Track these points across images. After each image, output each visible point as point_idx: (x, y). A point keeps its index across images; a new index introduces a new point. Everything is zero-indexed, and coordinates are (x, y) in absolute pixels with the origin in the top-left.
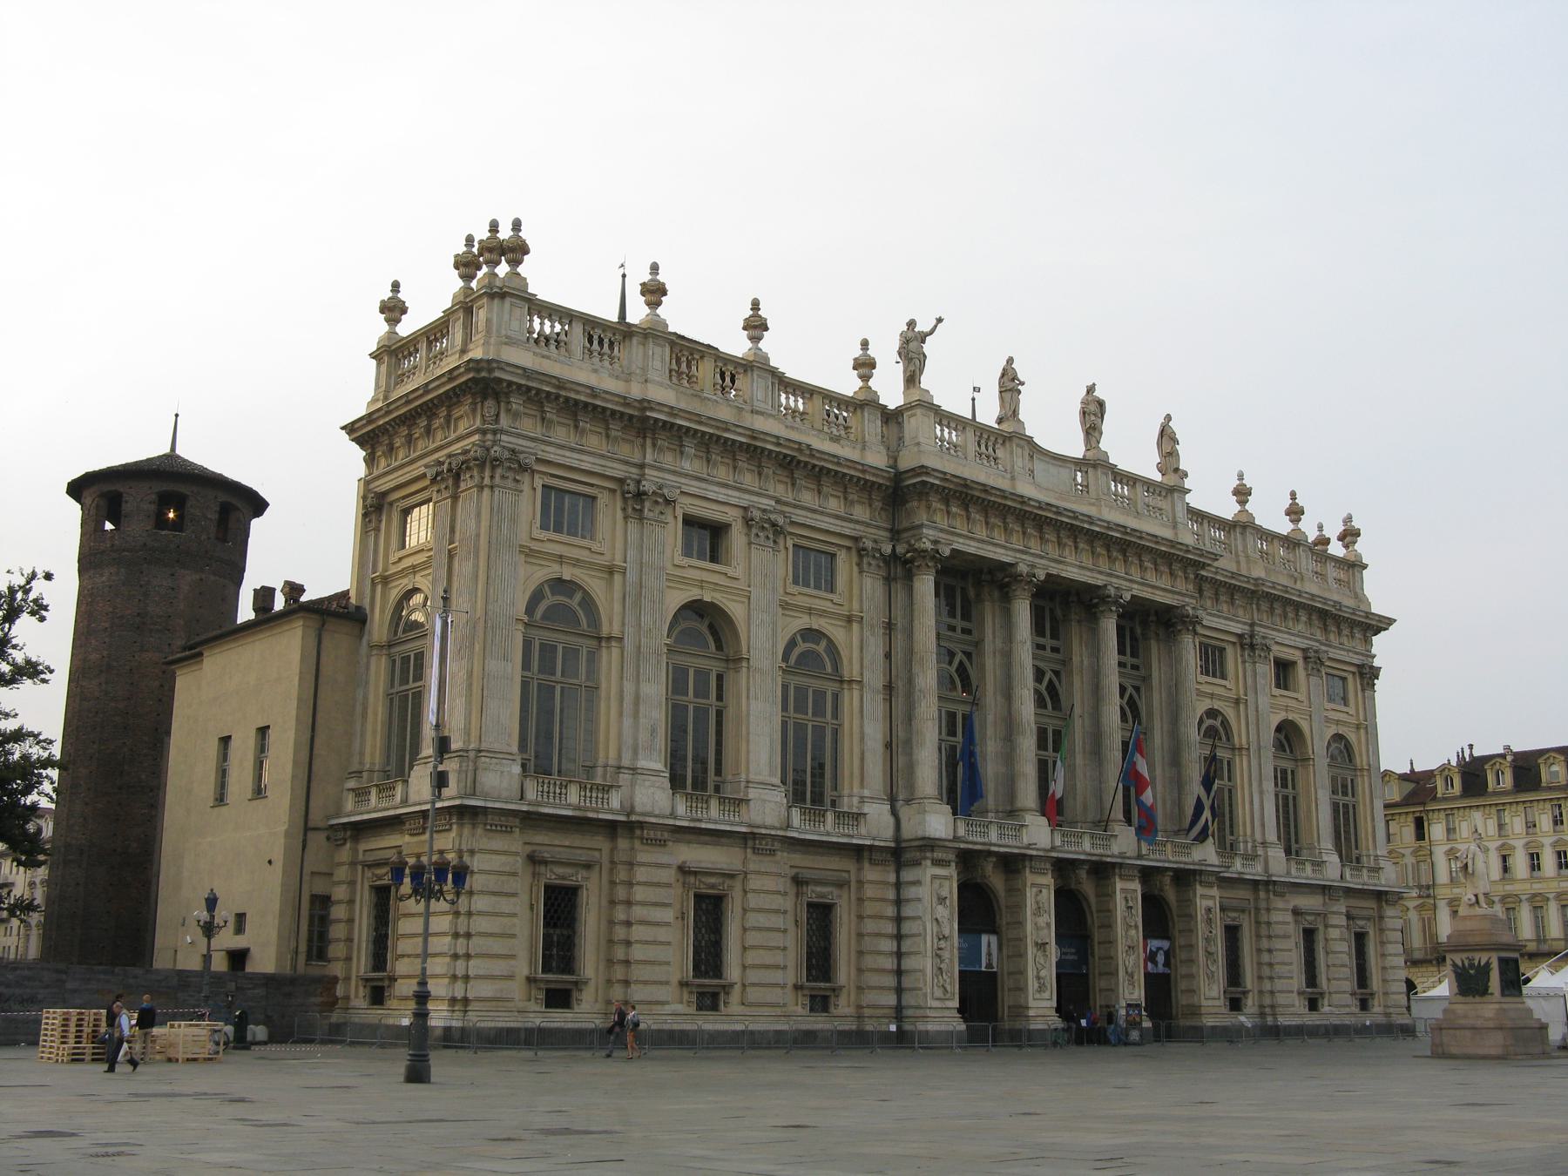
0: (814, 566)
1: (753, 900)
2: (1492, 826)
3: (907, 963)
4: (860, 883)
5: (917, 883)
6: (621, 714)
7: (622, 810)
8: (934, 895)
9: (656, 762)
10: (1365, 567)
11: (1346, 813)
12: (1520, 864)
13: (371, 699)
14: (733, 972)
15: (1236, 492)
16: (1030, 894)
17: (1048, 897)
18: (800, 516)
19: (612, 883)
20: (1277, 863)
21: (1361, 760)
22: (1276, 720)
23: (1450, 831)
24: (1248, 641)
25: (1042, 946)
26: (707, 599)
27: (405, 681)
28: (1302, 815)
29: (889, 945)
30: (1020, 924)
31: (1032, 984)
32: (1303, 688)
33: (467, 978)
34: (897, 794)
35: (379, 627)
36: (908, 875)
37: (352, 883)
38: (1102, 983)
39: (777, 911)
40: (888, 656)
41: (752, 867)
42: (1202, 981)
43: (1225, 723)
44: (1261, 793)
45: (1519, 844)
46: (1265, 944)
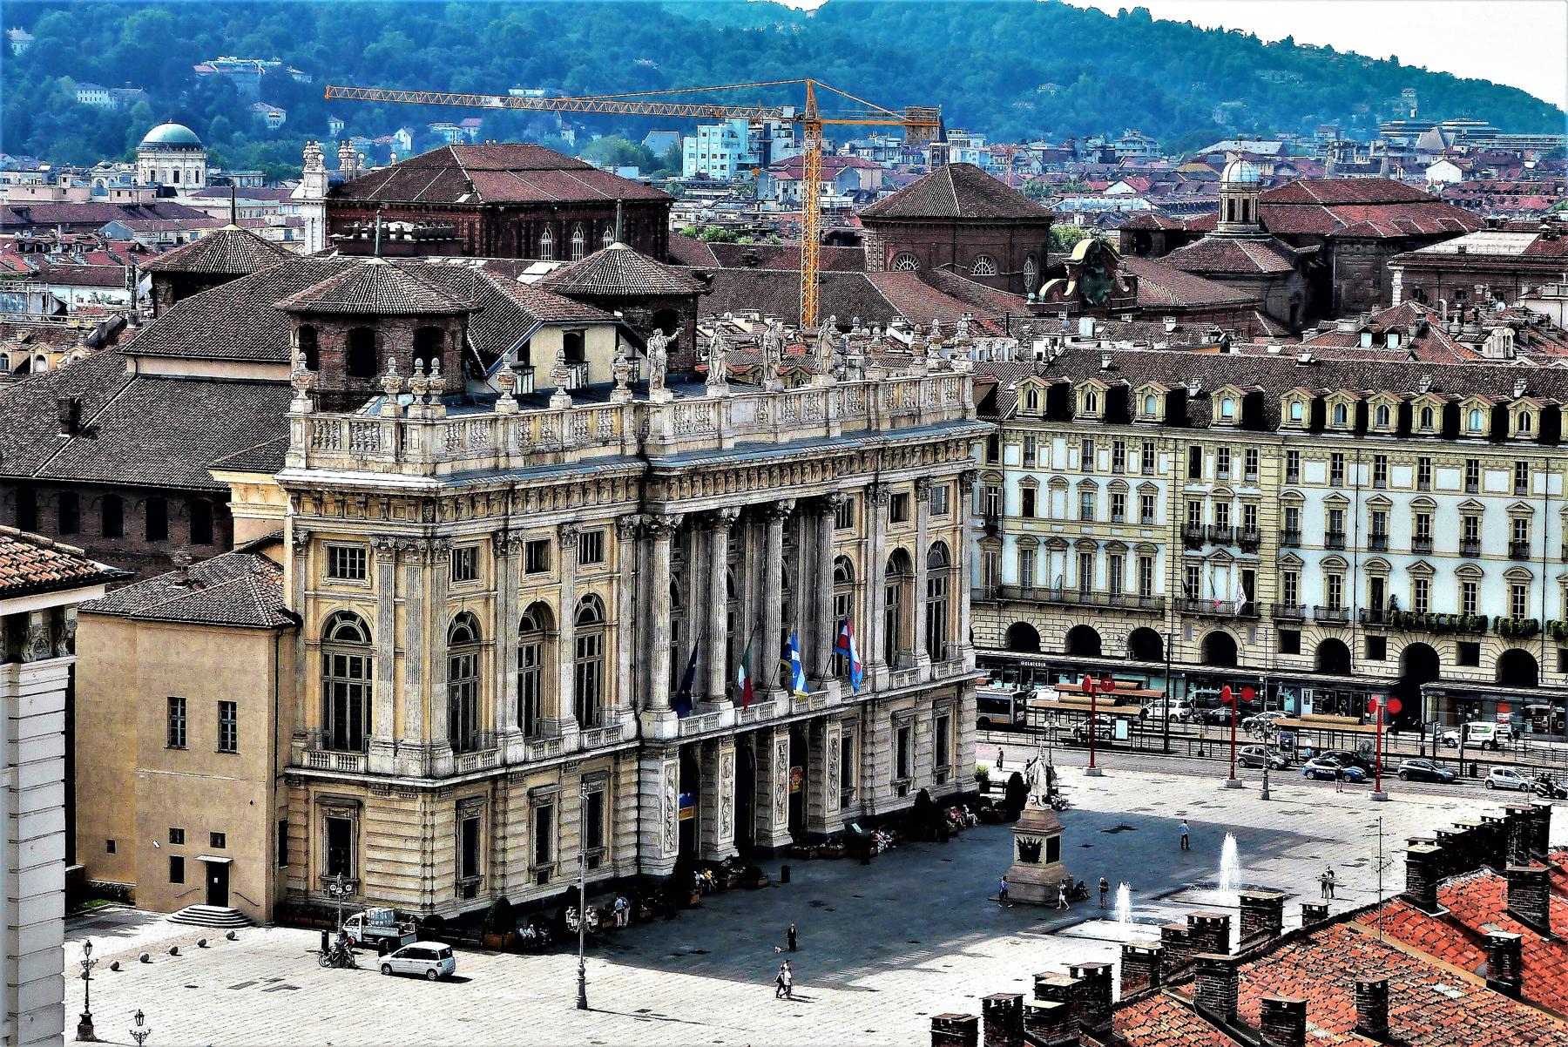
0: (591, 548)
2: (1076, 456)
3: (645, 827)
4: (617, 775)
5: (656, 771)
6: (495, 697)
8: (665, 778)
9: (512, 727)
11: (938, 610)
12: (1102, 510)
13: (309, 682)
14: (554, 856)
16: (721, 762)
17: (732, 760)
19: (495, 813)
23: (1028, 456)
25: (726, 799)
27: (340, 671)
28: (903, 623)
29: (634, 814)
30: (712, 784)
31: (720, 827)
33: (432, 892)
34: (642, 703)
35: (313, 628)
36: (646, 765)
37: (307, 814)
38: (758, 812)
40: (634, 599)
42: (827, 797)
44: (873, 621)
45: (1103, 482)
46: (868, 749)
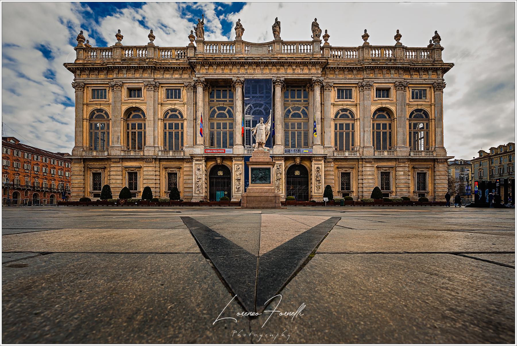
1: (145, 173)
7: (108, 156)
10: (442, 49)
15: (363, 37)
18: (164, 81)
20: (369, 153)
21: (432, 116)
22: (373, 108)
24: (360, 84)
26: (134, 106)
32: (395, 97)
39: (153, 175)
41: (145, 165)
43: (351, 113)
44: (364, 131)
46: (360, 177)
